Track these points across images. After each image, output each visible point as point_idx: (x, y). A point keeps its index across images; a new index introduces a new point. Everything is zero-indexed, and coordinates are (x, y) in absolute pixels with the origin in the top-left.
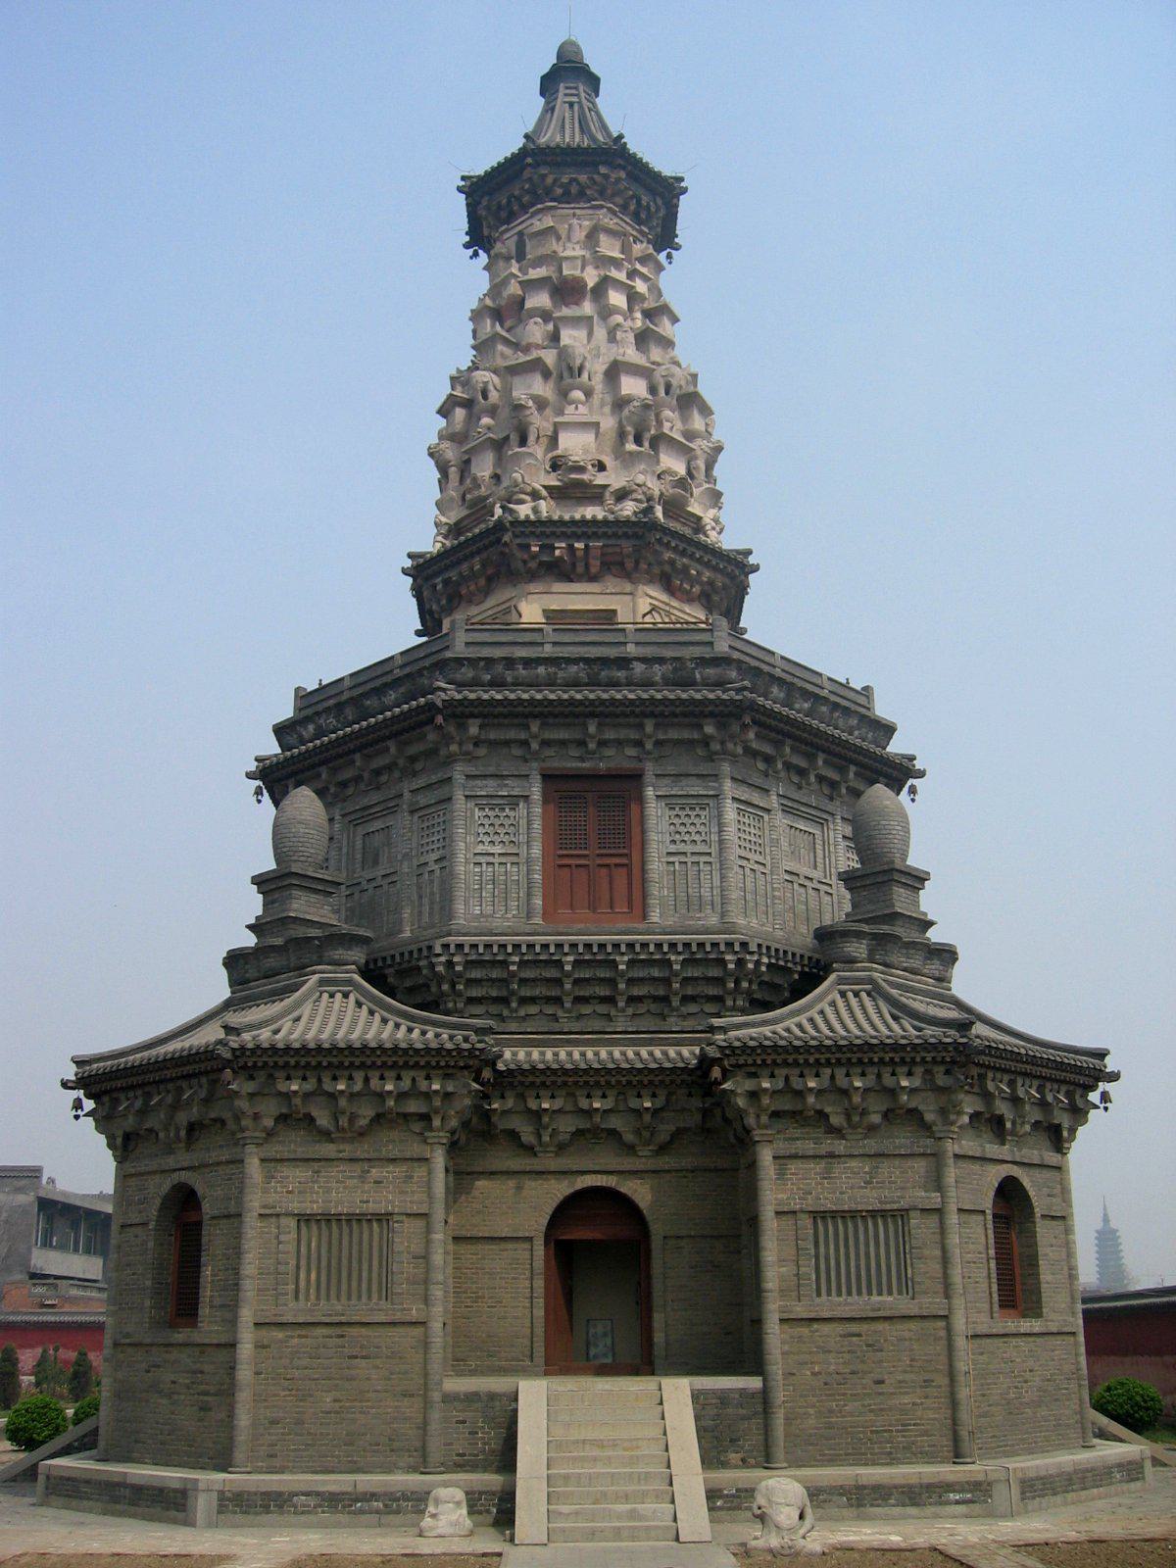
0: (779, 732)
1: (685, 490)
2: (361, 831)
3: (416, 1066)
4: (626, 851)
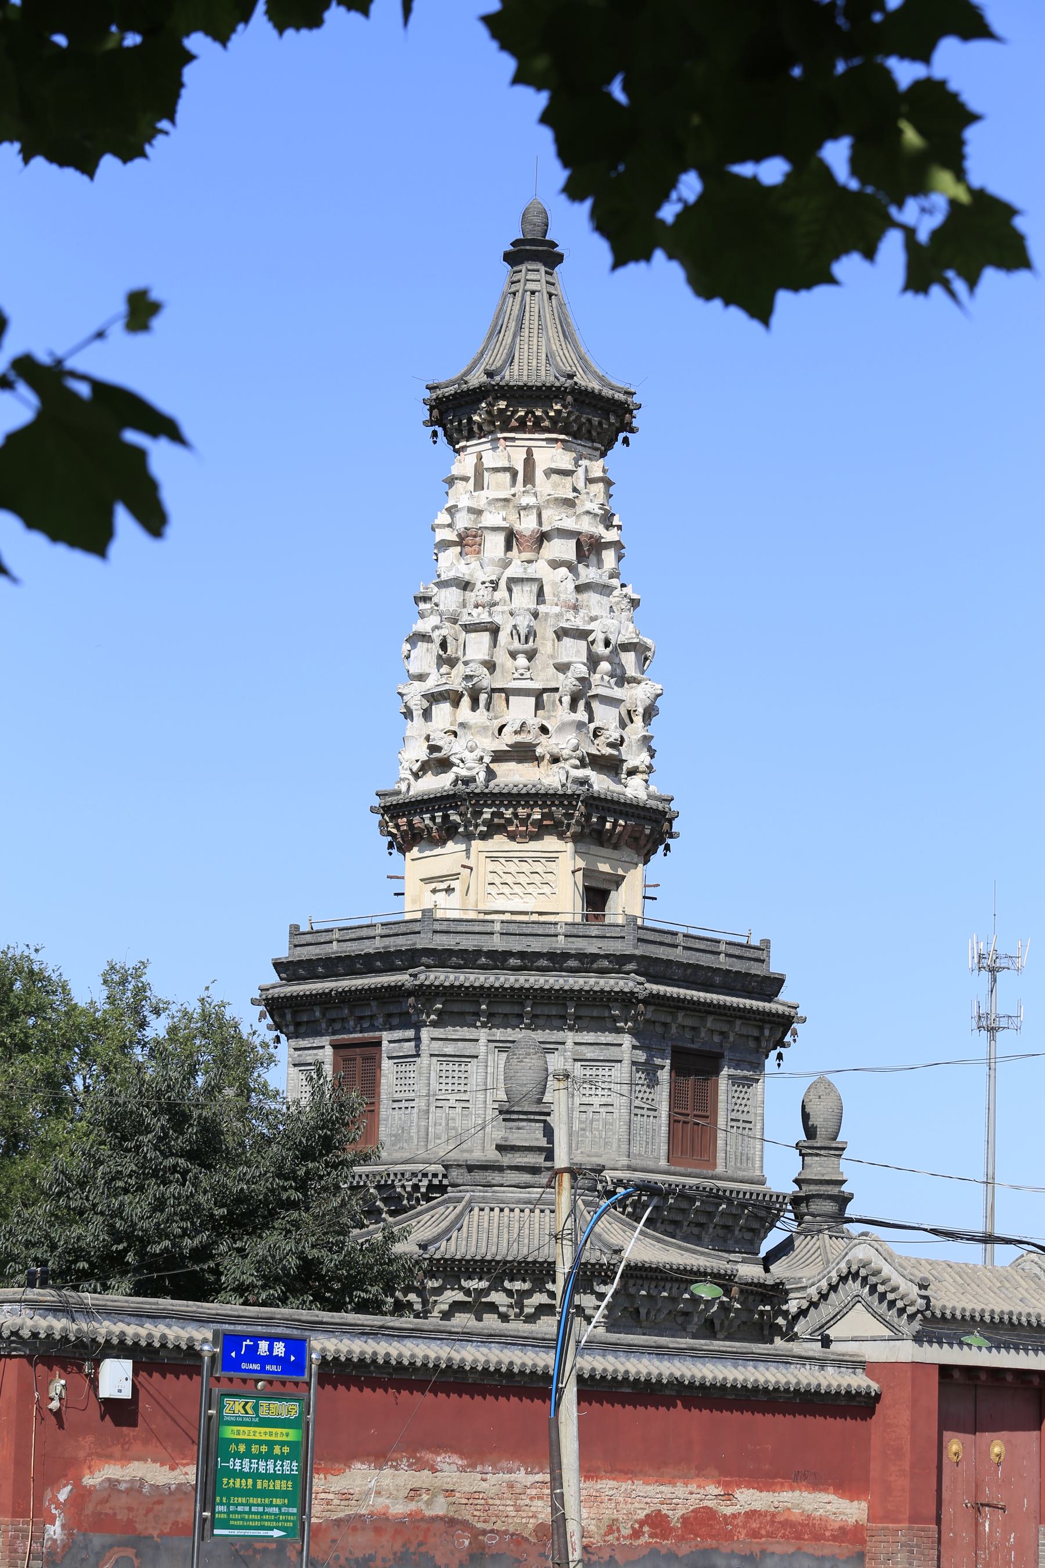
4: (708, 1114)
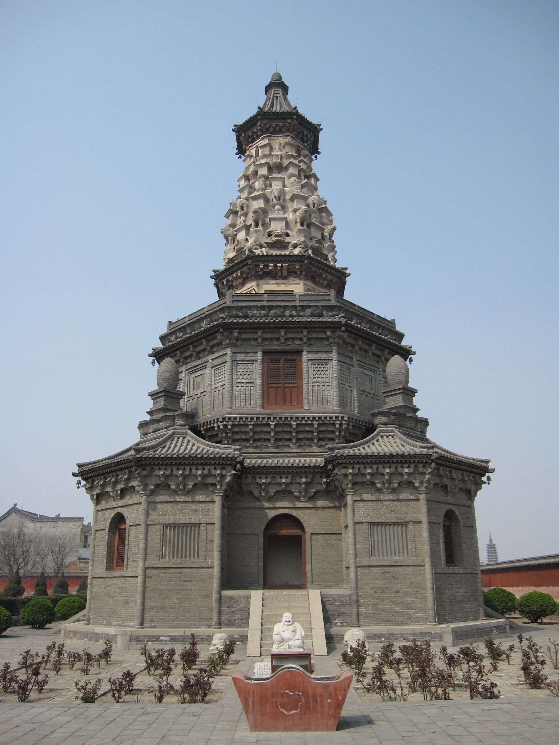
0: (357, 335)
1: (321, 244)
2: (193, 376)
3: (210, 464)
4: (296, 381)
